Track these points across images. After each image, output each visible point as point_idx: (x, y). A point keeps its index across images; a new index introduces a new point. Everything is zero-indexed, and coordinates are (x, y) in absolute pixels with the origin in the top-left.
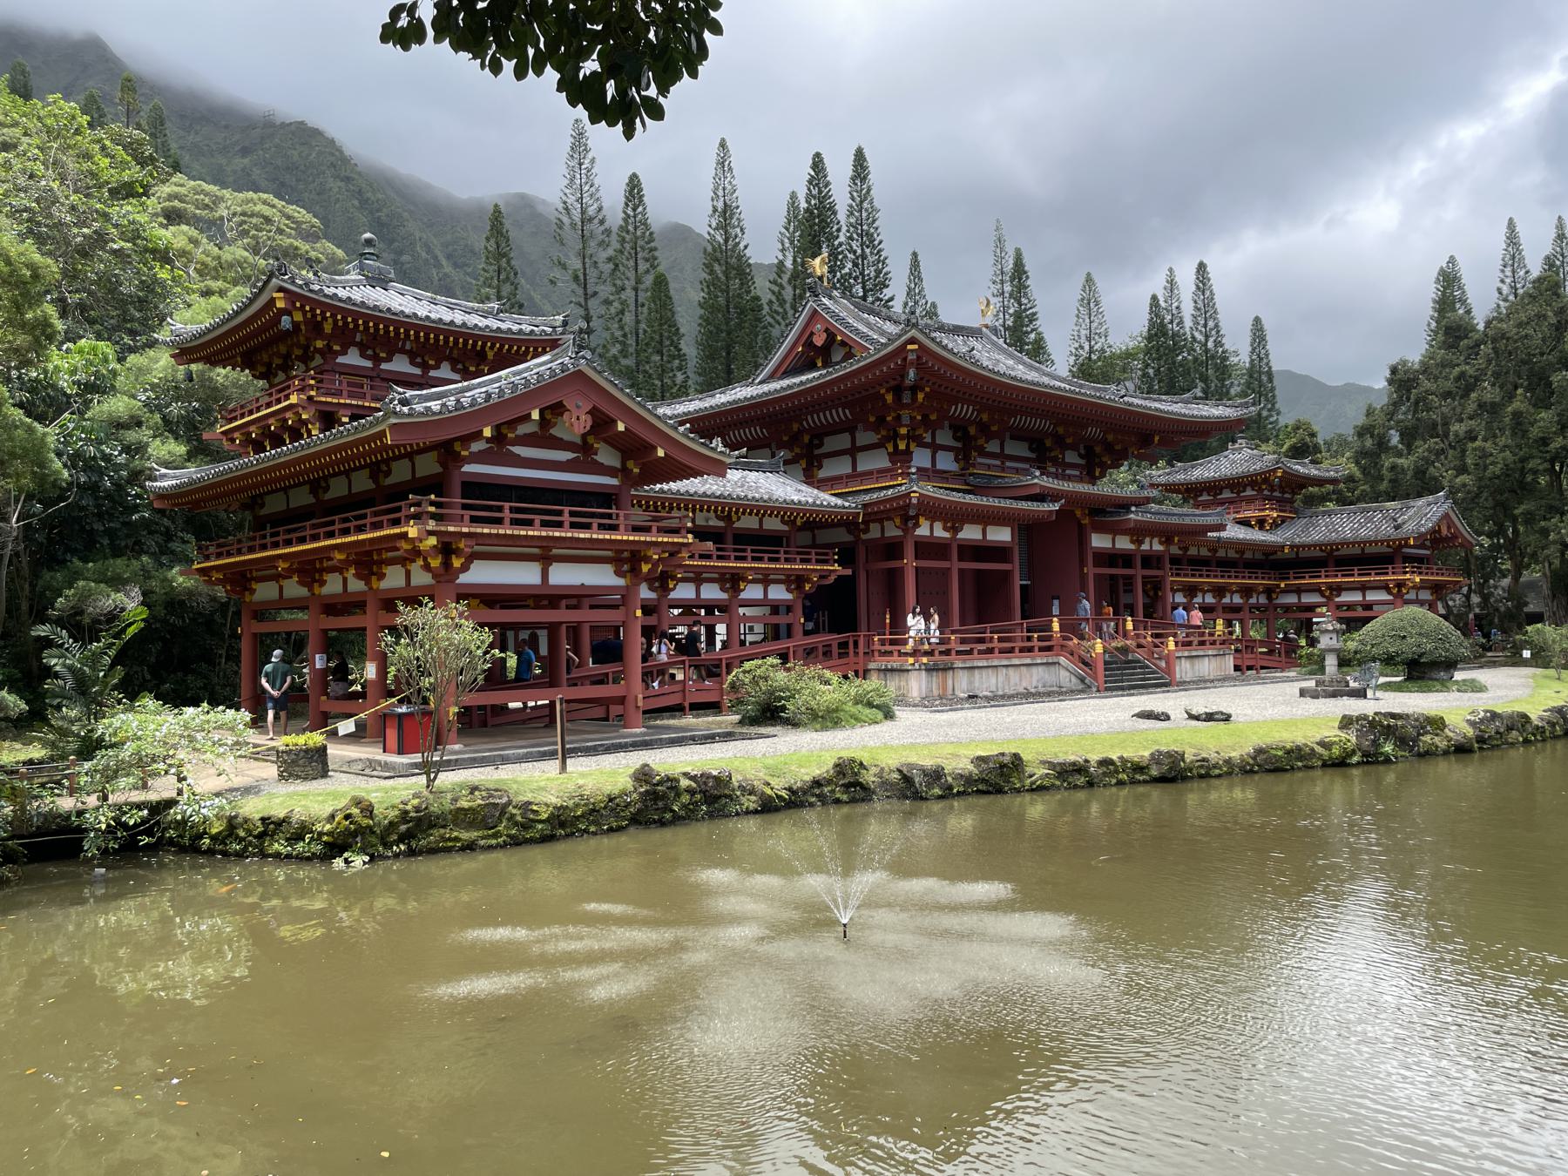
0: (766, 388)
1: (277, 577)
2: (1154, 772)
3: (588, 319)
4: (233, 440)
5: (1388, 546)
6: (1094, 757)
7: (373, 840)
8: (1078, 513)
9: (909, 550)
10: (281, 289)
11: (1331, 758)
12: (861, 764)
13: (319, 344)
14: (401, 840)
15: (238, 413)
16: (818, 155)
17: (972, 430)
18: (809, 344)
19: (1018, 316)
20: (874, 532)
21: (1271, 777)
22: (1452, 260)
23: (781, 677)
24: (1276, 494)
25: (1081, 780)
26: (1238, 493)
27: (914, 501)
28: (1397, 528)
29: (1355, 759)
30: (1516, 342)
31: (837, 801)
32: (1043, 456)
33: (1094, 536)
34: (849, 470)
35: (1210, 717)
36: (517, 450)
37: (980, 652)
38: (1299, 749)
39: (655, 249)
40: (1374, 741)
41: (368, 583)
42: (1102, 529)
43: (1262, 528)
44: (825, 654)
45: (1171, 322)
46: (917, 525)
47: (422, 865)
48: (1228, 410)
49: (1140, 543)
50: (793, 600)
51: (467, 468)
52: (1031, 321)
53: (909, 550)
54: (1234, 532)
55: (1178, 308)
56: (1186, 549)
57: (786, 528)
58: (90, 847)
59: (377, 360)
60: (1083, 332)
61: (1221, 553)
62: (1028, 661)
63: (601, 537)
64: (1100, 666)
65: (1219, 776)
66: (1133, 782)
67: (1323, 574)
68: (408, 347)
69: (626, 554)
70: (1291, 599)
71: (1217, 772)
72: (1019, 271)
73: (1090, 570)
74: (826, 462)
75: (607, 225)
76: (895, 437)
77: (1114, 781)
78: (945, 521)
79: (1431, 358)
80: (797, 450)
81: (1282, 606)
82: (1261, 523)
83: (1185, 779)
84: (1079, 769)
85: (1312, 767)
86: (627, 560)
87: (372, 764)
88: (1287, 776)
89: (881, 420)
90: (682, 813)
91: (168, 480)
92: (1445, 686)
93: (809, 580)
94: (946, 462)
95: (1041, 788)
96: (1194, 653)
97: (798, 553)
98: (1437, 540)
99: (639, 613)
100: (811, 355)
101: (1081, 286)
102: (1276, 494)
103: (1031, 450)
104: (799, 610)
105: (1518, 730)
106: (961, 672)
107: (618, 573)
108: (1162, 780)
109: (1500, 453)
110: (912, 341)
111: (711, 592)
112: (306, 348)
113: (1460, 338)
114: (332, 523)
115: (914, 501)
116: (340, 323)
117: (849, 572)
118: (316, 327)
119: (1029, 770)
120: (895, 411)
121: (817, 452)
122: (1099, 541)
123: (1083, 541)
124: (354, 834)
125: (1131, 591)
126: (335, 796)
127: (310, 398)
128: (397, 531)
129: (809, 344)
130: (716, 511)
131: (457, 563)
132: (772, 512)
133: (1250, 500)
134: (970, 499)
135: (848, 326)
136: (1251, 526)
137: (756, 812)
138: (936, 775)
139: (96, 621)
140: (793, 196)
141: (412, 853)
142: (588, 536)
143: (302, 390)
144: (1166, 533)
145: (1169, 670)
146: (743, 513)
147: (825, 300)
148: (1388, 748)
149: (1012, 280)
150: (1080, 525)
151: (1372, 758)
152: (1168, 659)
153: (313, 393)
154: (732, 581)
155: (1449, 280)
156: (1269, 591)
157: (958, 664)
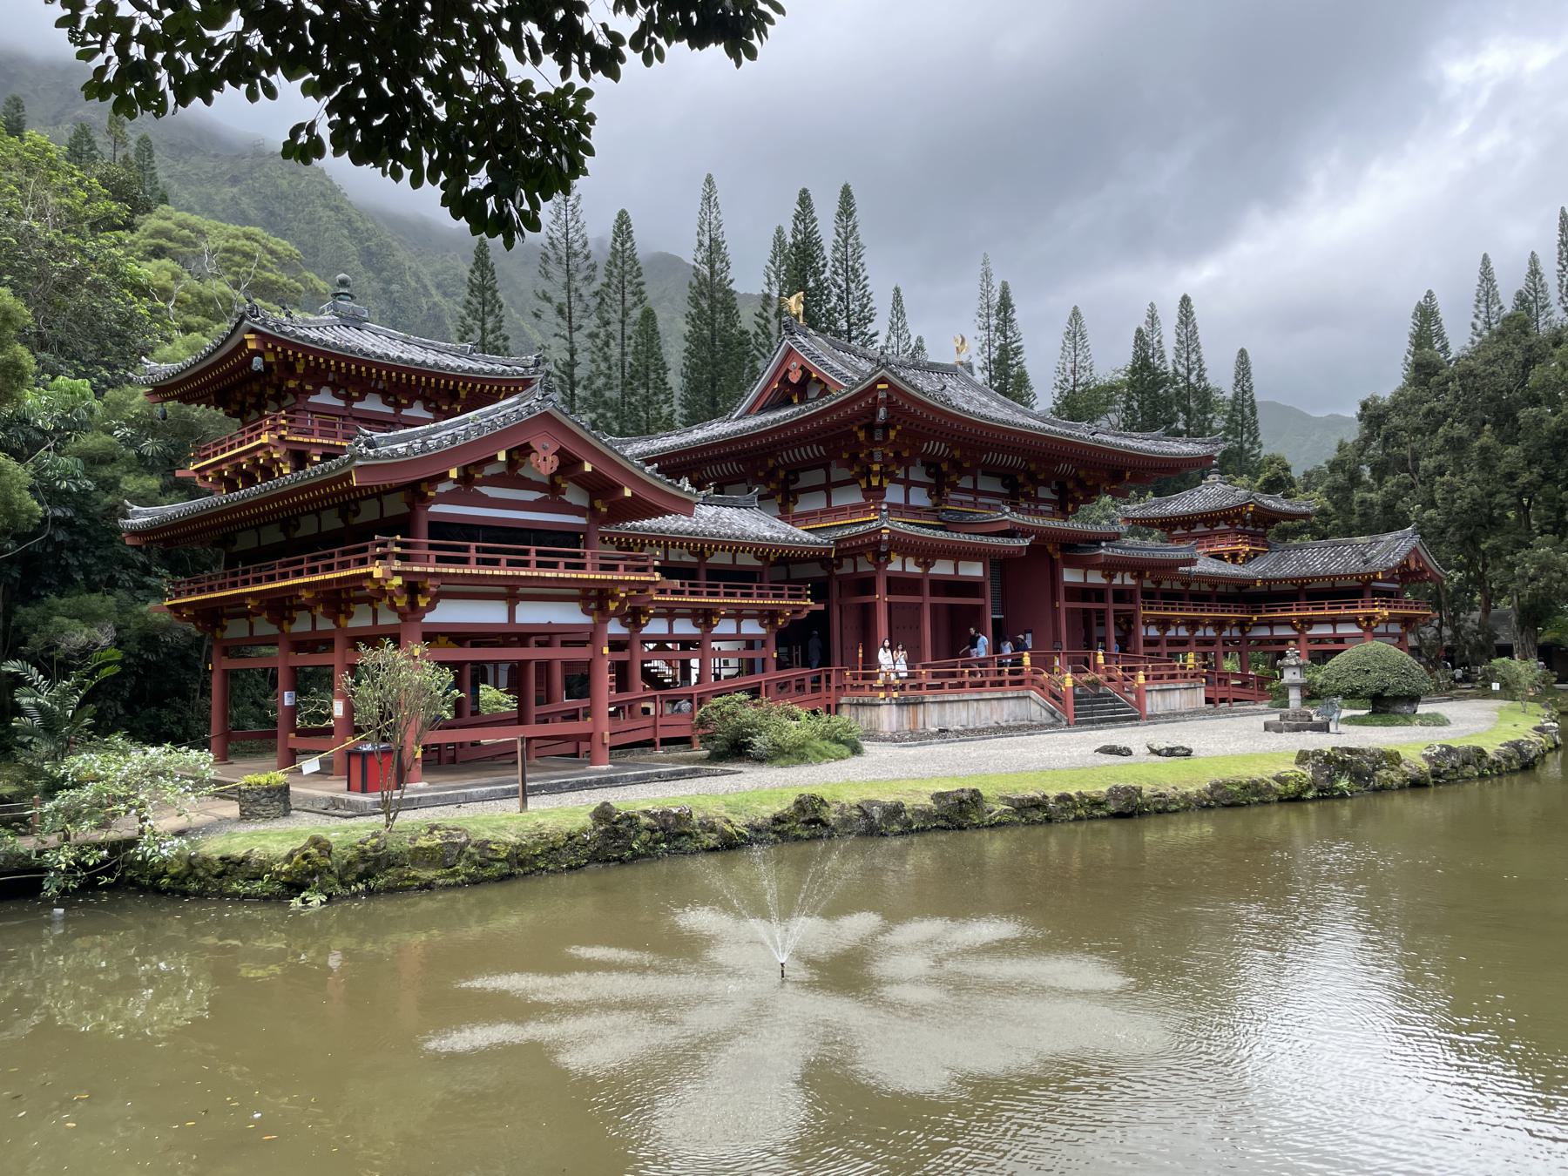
0: (741, 424)
1: (247, 615)
2: (1112, 808)
3: (572, 352)
4: (206, 478)
5: (1358, 580)
6: (1053, 793)
7: (331, 879)
8: (1050, 548)
9: (881, 585)
10: (252, 331)
11: (1286, 793)
12: (822, 801)
13: (292, 384)
14: (359, 879)
15: (211, 451)
16: (805, 191)
17: (945, 467)
18: (785, 381)
19: (1003, 349)
20: (847, 568)
21: (1228, 812)
22: (1430, 295)
23: (749, 713)
24: (1249, 528)
25: (1040, 815)
26: (1212, 527)
27: (885, 537)
28: (1366, 562)
29: (1310, 794)
30: (1483, 379)
31: (797, 838)
32: (1015, 494)
34: (823, 505)
35: (1171, 752)
36: (485, 490)
37: (951, 686)
38: (1255, 784)
39: (643, 284)
40: (1329, 776)
41: (336, 622)
42: (1073, 564)
43: (1234, 561)
44: (798, 688)
45: (1153, 356)
46: (889, 561)
47: (382, 906)
48: (1198, 447)
49: (1112, 577)
50: (767, 635)
51: (434, 508)
52: (1016, 355)
53: (881, 585)
54: (1206, 566)
55: (1159, 342)
56: (1159, 583)
57: (759, 563)
58: (50, 889)
59: (349, 399)
60: (1069, 366)
61: (1194, 587)
62: (999, 695)
63: (567, 576)
64: (1070, 699)
65: (1176, 811)
66: (1091, 818)
67: (1294, 607)
68: (380, 386)
69: (593, 593)
70: (1264, 632)
71: (1174, 807)
72: (1005, 305)
73: (1062, 605)
74: (801, 497)
75: (591, 261)
76: (868, 473)
77: (1072, 816)
78: (916, 556)
79: (1401, 395)
80: (773, 486)
81: (1255, 639)
82: (1234, 557)
83: (1142, 814)
84: (1038, 804)
85: (1268, 803)
86: (596, 598)
87: (334, 803)
88: (1244, 811)
89: (854, 458)
90: (642, 850)
91: (140, 517)
92: (1407, 720)
93: (782, 615)
94: (919, 498)
95: (1000, 824)
96: (1165, 687)
97: (772, 588)
98: (1406, 574)
99: (606, 650)
100: (788, 391)
101: (1067, 320)
102: (1249, 528)
103: (1004, 485)
104: (772, 643)
105: (1474, 765)
106: (932, 706)
107: (586, 611)
108: (1119, 815)
109: (1468, 487)
110: (882, 380)
111: (684, 628)
112: (278, 387)
113: (1430, 375)
114: (301, 562)
115: (885, 537)
116: (312, 364)
117: (821, 607)
118: (288, 367)
119: (988, 806)
120: (868, 448)
121: (792, 487)
122: (1070, 576)
123: (1055, 576)
124: (312, 874)
125: (1103, 624)
126: (294, 835)
127: (281, 438)
128: (363, 571)
129: (785, 381)
131: (422, 603)
132: (744, 548)
133: (1223, 534)
134: (940, 534)
135: (822, 363)
136: (1225, 560)
137: (715, 849)
138: (895, 811)
139: (68, 656)
140: (780, 231)
141: (370, 892)
142: (554, 575)
143: (273, 429)
144: (1138, 568)
145: (1140, 704)
146: (716, 549)
147: (800, 338)
148: (1344, 783)
149: (998, 314)
150: (1052, 560)
151: (1327, 794)
152: (1138, 692)
153: (284, 433)
154: (705, 617)
155: (1426, 315)
156: (1242, 624)
157: (929, 698)
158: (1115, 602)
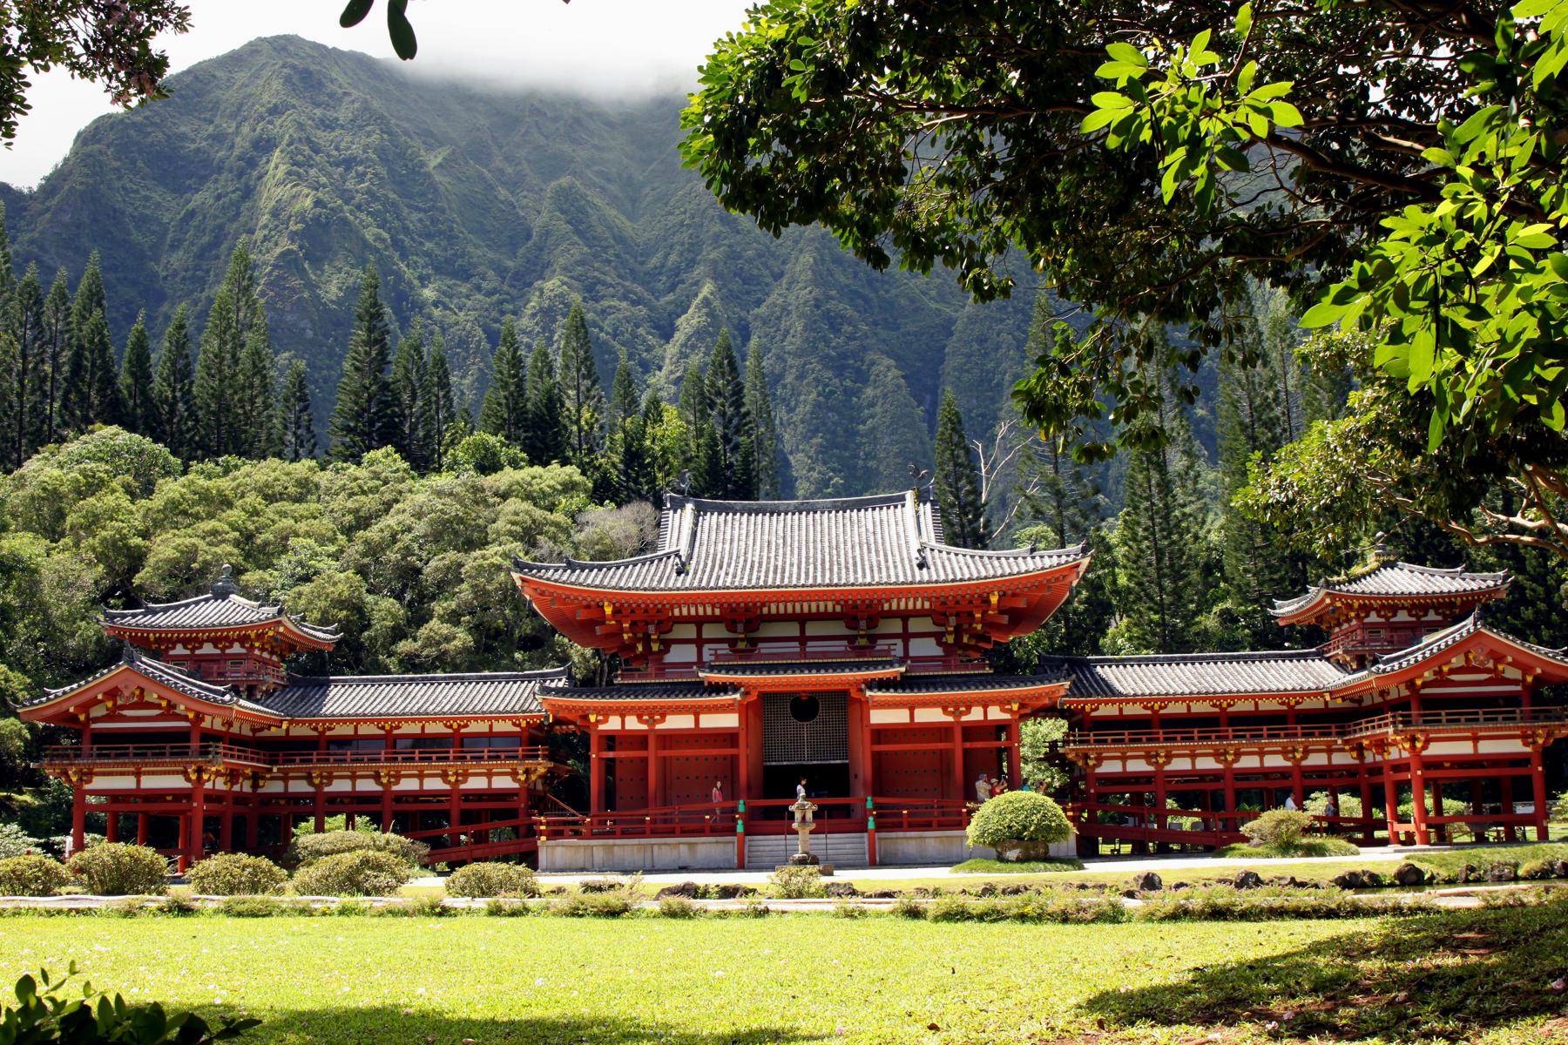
33: (873, 712)
49: (959, 714)
51: (94, 726)
158: (965, 739)
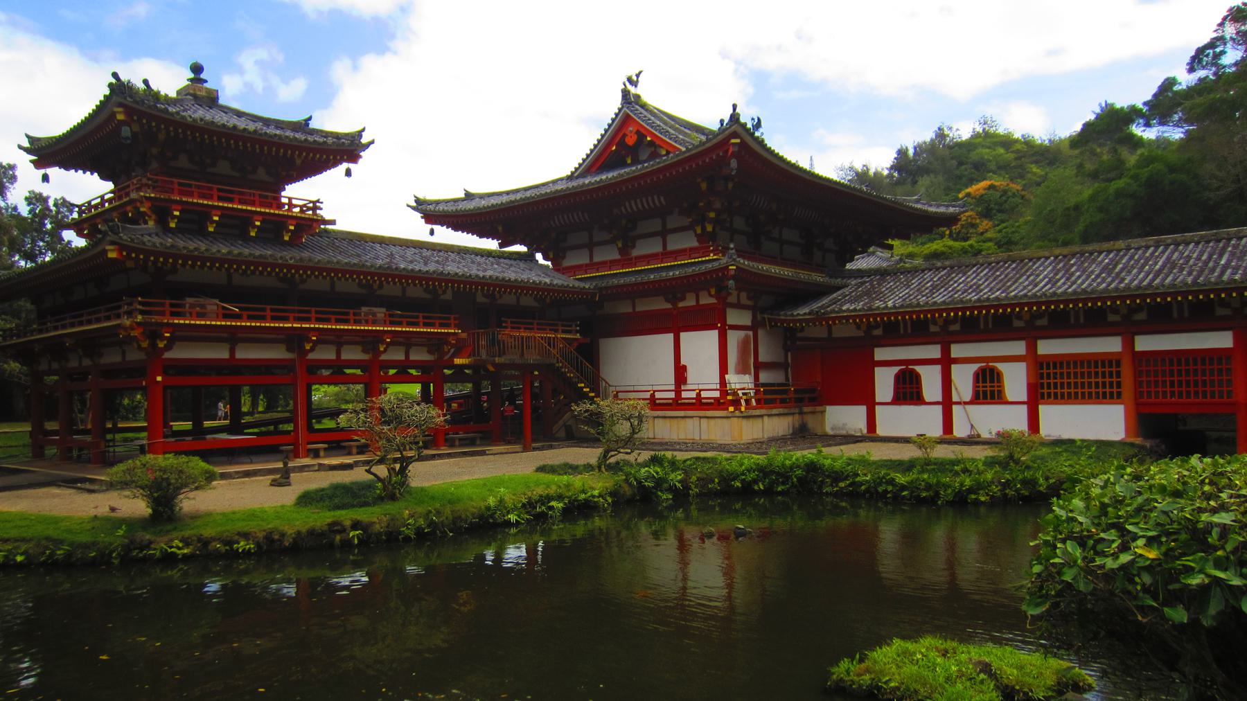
114: (82, 315)
116: (172, 134)
128: (118, 322)
130: (482, 289)
146: (505, 292)
